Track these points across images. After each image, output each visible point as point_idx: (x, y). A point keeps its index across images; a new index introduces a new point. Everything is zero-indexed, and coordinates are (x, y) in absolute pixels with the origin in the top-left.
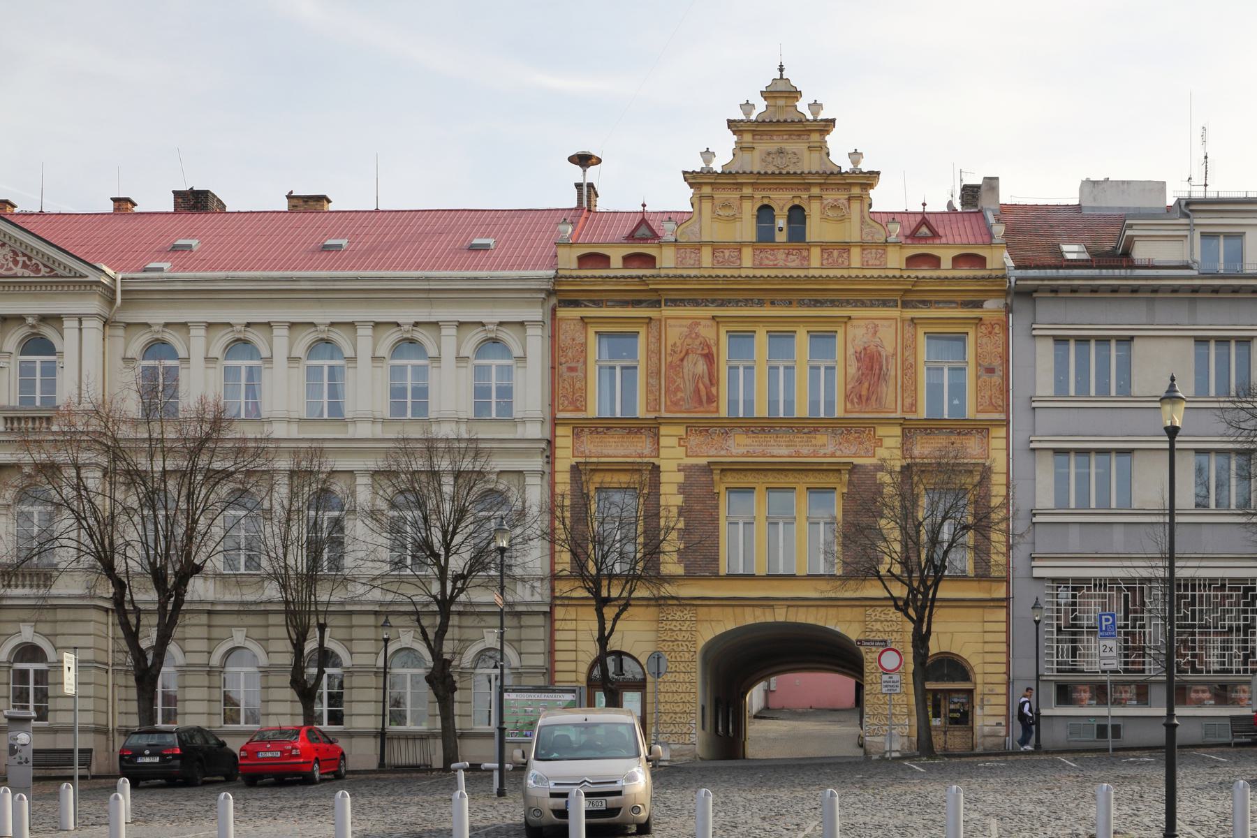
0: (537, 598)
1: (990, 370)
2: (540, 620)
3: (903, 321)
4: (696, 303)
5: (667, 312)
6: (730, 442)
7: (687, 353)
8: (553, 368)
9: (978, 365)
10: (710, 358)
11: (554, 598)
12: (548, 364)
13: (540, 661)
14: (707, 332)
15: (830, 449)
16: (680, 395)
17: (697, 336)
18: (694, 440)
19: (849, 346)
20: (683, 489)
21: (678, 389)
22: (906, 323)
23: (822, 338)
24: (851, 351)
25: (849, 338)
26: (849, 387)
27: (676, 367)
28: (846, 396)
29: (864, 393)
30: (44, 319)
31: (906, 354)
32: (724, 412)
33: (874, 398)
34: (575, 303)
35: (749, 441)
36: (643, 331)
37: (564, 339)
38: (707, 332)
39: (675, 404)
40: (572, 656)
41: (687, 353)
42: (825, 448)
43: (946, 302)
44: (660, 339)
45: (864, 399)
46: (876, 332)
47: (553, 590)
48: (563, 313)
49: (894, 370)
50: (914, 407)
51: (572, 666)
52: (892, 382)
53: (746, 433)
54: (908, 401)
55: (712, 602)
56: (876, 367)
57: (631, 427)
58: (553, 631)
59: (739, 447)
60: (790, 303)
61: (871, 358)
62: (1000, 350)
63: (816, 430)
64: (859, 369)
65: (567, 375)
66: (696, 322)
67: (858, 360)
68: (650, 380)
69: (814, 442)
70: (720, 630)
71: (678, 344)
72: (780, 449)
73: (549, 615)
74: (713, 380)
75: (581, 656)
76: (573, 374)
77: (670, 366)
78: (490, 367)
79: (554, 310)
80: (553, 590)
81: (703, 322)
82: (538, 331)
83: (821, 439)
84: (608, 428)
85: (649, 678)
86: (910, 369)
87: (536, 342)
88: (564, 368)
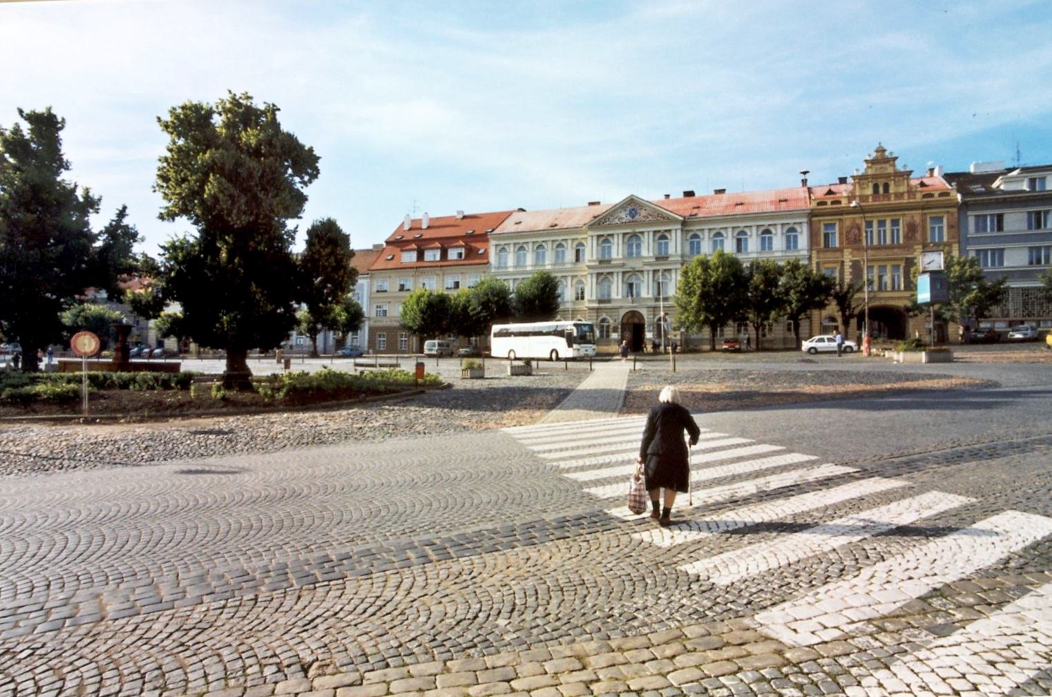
10: (859, 229)
14: (858, 221)
18: (855, 252)
20: (851, 267)
30: (666, 231)
66: (854, 219)
86: (924, 228)
87: (805, 228)
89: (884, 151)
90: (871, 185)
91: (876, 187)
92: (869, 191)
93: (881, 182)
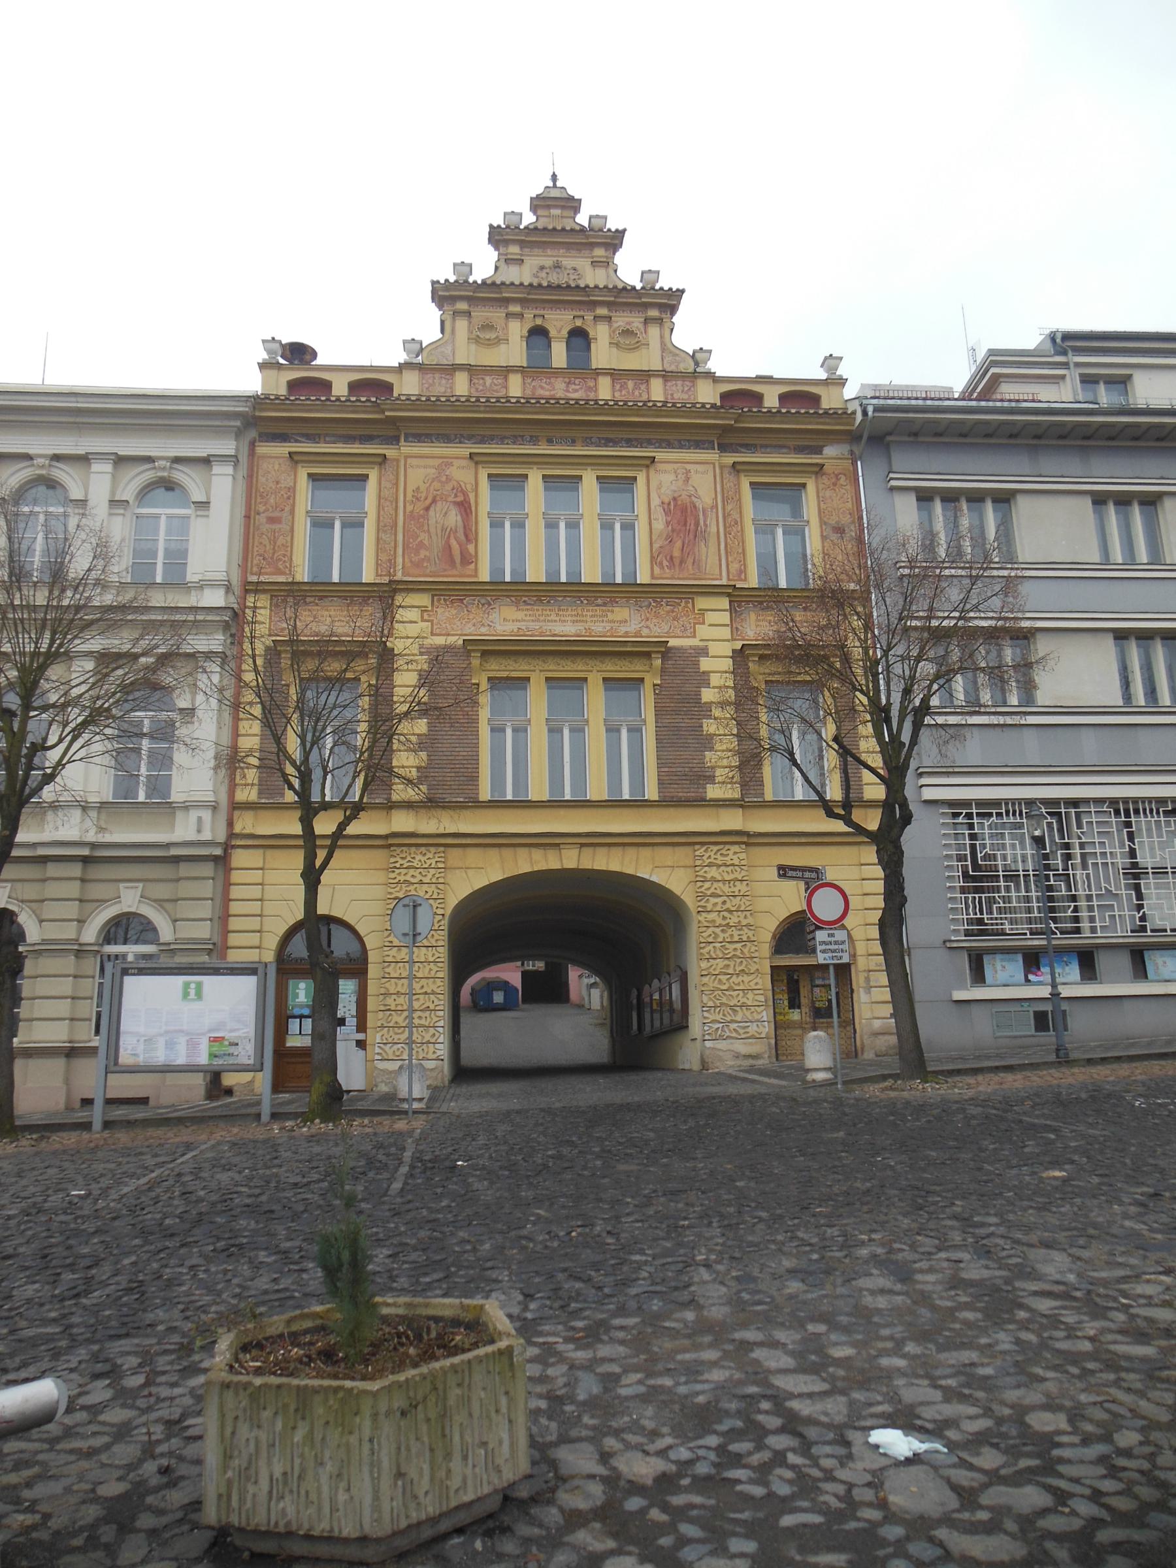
0: (207, 835)
1: (840, 530)
2: (208, 870)
3: (722, 467)
4: (447, 439)
5: (407, 448)
6: (494, 616)
7: (434, 501)
8: (247, 517)
9: (822, 523)
10: (465, 507)
11: (231, 835)
12: (240, 512)
13: (203, 931)
15: (632, 627)
16: (423, 553)
17: (449, 479)
18: (444, 613)
19: (654, 495)
21: (421, 545)
22: (726, 471)
23: (617, 485)
24: (656, 501)
25: (654, 484)
26: (656, 546)
27: (417, 519)
28: (652, 558)
29: (677, 553)
31: (729, 508)
32: (485, 576)
33: (690, 560)
34: (283, 438)
35: (520, 615)
36: (373, 475)
37: (264, 481)
38: (462, 473)
39: (418, 565)
40: (254, 923)
41: (434, 501)
42: (626, 623)
43: (775, 446)
44: (397, 484)
45: (677, 562)
46: (687, 479)
47: (230, 824)
48: (263, 449)
49: (714, 525)
50: (742, 572)
51: (254, 939)
52: (712, 542)
53: (517, 604)
54: (735, 567)
55: (469, 841)
56: (691, 521)
57: (352, 593)
58: (227, 885)
59: (507, 622)
60: (574, 441)
61: (684, 510)
62: (849, 505)
63: (613, 601)
64: (668, 523)
65: (265, 527)
67: (667, 512)
68: (382, 535)
69: (610, 616)
70: (480, 881)
71: (423, 487)
72: (564, 625)
73: (222, 862)
74: (470, 535)
75: (269, 924)
76: (276, 527)
77: (410, 517)
78: (157, 517)
79: (252, 445)
80: (230, 824)
81: (456, 463)
82: (229, 469)
83: (621, 613)
84: (321, 598)
85: (372, 957)
86: (733, 526)
87: (223, 487)
88: (262, 519)
89: (572, 204)
90: (517, 331)
91: (538, 333)
92: (514, 351)
93: (559, 322)
